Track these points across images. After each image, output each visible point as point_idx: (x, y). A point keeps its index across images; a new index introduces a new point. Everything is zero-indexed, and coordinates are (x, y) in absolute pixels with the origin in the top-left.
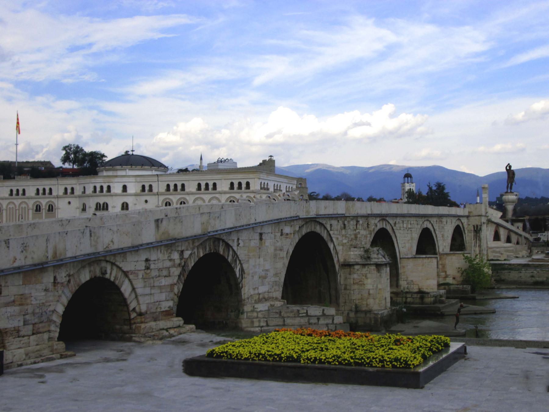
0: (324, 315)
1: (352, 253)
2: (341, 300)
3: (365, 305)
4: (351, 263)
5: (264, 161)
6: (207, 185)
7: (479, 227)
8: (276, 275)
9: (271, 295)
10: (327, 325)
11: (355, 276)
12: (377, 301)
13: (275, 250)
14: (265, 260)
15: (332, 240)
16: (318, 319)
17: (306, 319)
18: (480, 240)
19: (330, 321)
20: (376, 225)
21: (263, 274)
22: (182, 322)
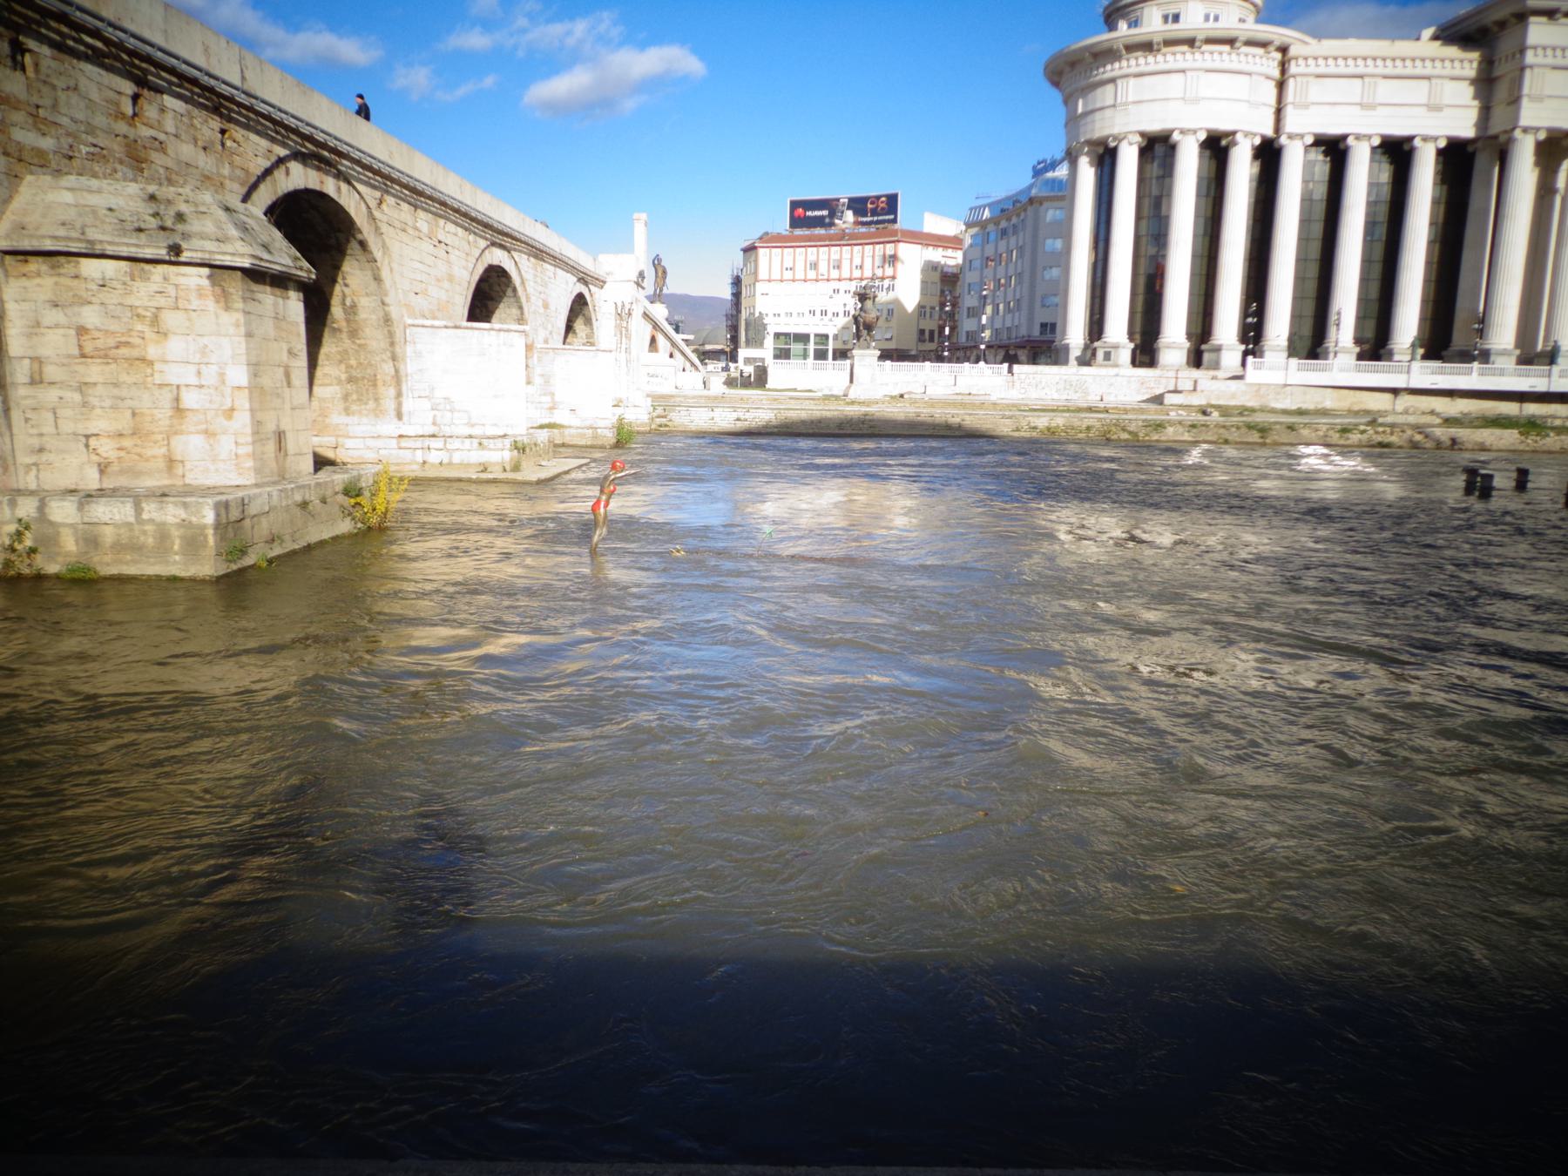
1: (68, 197)
3: (161, 464)
4: (49, 245)
7: (627, 306)
11: (90, 316)
12: (226, 445)
18: (628, 337)
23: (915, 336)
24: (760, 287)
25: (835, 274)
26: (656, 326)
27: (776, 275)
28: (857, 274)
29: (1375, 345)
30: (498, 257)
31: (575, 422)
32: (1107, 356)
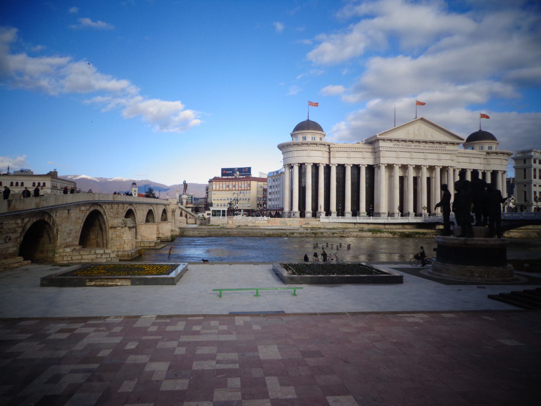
0: (105, 253)
2: (109, 246)
5: (51, 172)
6: (17, 184)
8: (76, 232)
9: (73, 243)
10: (106, 258)
11: (117, 233)
12: (129, 246)
13: (76, 219)
14: (71, 224)
15: (105, 214)
16: (102, 255)
17: (95, 256)
19: (108, 256)
20: (127, 207)
21: (69, 232)
22: (23, 259)
23: (256, 205)
24: (213, 192)
25: (234, 189)
26: (182, 209)
27: (218, 189)
28: (240, 189)
29: (355, 212)
30: (151, 208)
31: (163, 236)
32: (294, 215)
